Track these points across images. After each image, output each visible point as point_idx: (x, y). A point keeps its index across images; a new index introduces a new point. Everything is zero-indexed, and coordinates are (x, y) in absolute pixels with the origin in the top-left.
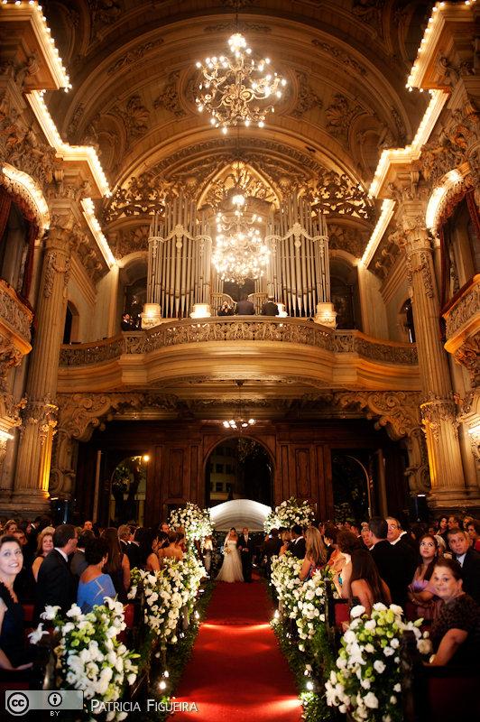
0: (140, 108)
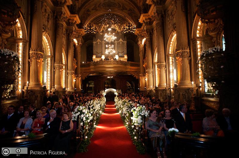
0: (89, 11)
